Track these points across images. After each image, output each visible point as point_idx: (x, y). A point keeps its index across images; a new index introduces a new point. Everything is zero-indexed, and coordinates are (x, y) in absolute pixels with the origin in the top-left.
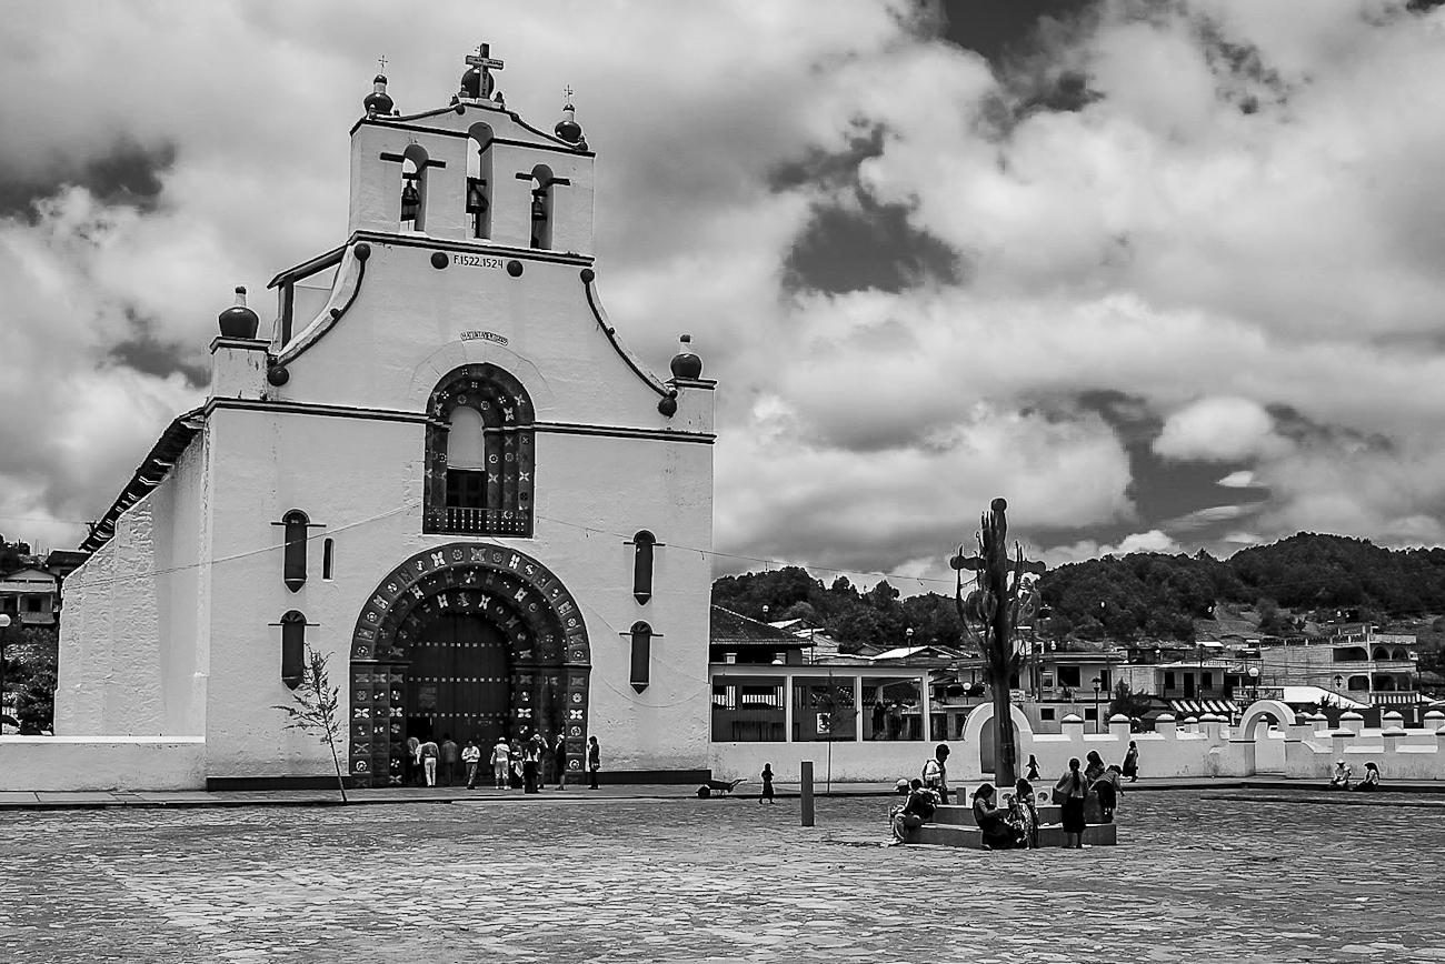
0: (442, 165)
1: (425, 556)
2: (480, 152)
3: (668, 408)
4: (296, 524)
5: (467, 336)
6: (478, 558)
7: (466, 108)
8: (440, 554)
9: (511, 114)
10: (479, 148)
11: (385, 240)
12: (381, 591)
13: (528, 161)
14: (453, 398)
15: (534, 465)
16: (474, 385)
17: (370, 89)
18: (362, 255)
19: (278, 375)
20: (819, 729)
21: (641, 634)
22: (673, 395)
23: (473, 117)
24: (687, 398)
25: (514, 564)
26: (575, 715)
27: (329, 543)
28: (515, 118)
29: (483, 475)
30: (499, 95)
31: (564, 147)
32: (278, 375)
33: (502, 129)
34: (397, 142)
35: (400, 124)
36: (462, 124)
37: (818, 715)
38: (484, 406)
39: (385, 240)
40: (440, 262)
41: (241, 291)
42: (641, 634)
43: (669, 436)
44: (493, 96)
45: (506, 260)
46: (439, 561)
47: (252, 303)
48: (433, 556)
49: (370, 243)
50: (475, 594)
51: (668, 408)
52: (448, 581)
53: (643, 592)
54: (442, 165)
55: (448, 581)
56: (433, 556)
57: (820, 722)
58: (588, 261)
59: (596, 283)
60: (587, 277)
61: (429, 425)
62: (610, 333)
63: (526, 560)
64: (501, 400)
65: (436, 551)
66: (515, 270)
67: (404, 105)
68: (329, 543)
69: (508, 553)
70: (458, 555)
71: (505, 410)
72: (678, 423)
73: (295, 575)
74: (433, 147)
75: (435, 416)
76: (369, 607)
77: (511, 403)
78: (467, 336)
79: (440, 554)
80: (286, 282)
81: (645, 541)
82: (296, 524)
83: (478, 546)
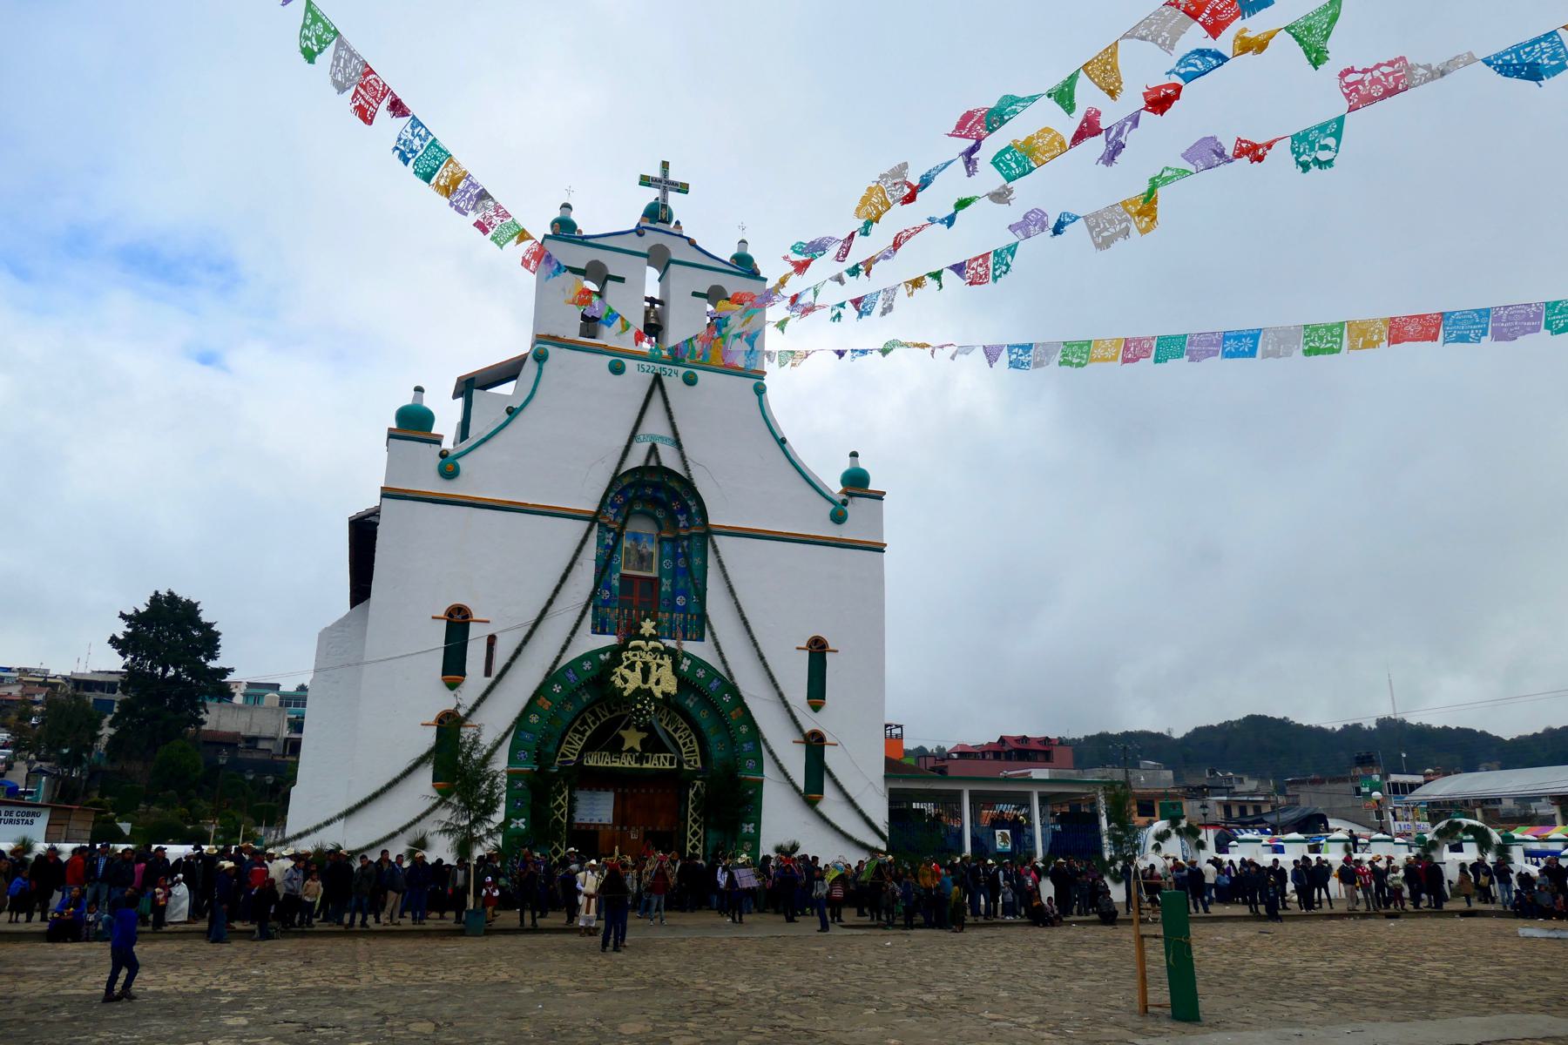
0: (621, 280)
2: (660, 280)
3: (838, 517)
7: (646, 230)
9: (688, 239)
10: (659, 275)
13: (705, 282)
14: (629, 502)
15: (707, 567)
17: (557, 214)
18: (540, 358)
19: (449, 469)
20: (998, 847)
22: (845, 503)
23: (652, 239)
24: (857, 507)
26: (748, 828)
27: (492, 640)
28: (692, 243)
29: (654, 583)
30: (678, 223)
32: (449, 469)
33: (678, 251)
35: (584, 241)
36: (641, 246)
37: (998, 832)
38: (660, 514)
41: (419, 390)
44: (673, 224)
47: (428, 402)
49: (548, 347)
51: (838, 517)
54: (621, 280)
57: (999, 839)
58: (760, 375)
59: (771, 395)
60: (760, 390)
62: (782, 442)
64: (675, 506)
65: (603, 650)
67: (586, 226)
68: (492, 640)
71: (679, 516)
72: (844, 532)
74: (614, 263)
77: (685, 509)
80: (468, 387)
82: (458, 622)
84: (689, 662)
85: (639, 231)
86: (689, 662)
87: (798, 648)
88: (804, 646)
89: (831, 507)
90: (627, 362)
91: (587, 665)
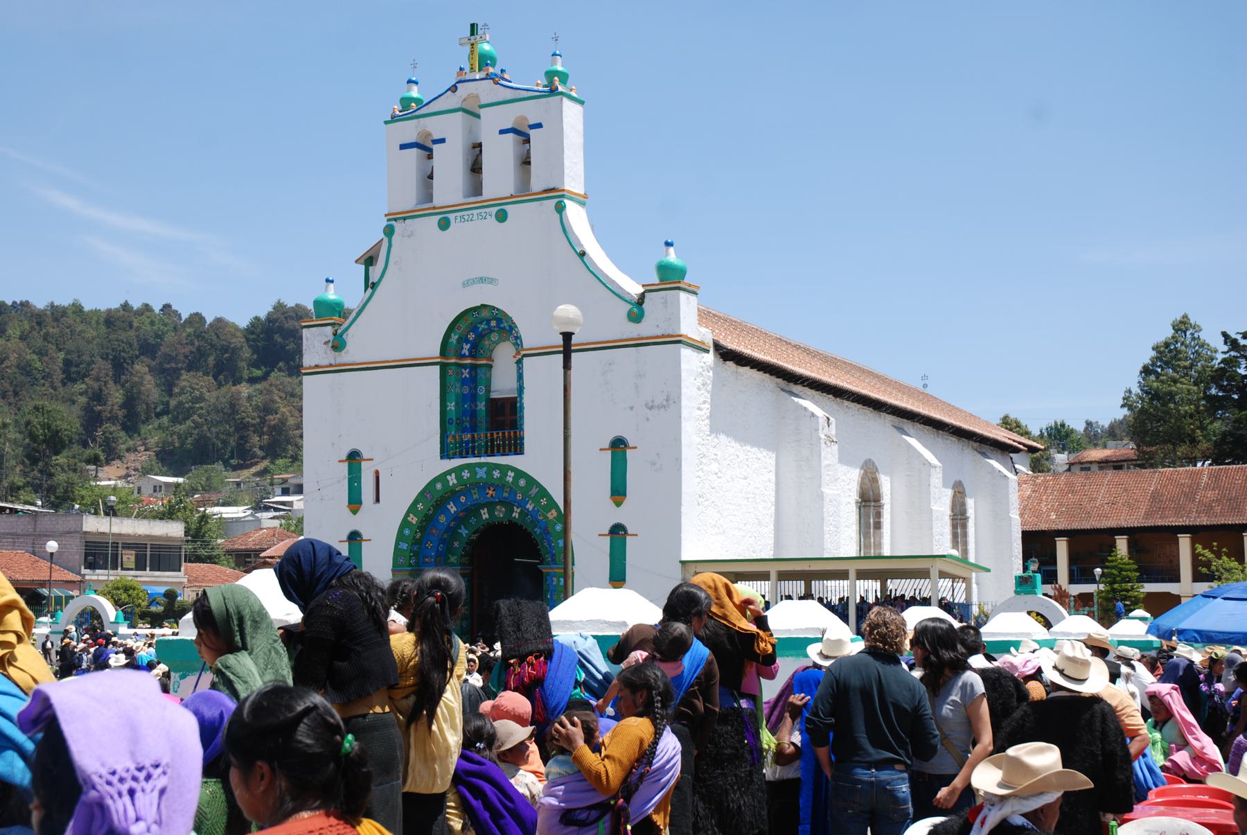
1: (442, 478)
4: (354, 458)
5: (466, 284)
6: (481, 473)
8: (453, 475)
11: (405, 216)
12: (412, 509)
13: (508, 116)
14: (481, 336)
16: (493, 323)
21: (618, 531)
25: (511, 474)
27: (377, 473)
31: (538, 94)
32: (338, 345)
34: (409, 131)
39: (405, 216)
40: (444, 225)
42: (618, 531)
43: (639, 344)
45: (496, 209)
46: (452, 480)
48: (448, 477)
49: (393, 223)
50: (509, 505)
52: (475, 497)
53: (618, 492)
55: (475, 497)
56: (448, 477)
60: (560, 208)
61: (444, 368)
63: (520, 474)
65: (449, 472)
66: (502, 217)
68: (377, 473)
69: (505, 469)
70: (466, 474)
72: (645, 329)
73: (355, 502)
74: (435, 126)
75: (464, 357)
76: (405, 523)
78: (466, 284)
79: (453, 475)
81: (618, 445)
83: (480, 465)
84: (513, 474)
85: (454, 89)
86: (513, 474)
87: (601, 450)
88: (607, 447)
89: (630, 306)
90: (452, 217)
91: (439, 486)
